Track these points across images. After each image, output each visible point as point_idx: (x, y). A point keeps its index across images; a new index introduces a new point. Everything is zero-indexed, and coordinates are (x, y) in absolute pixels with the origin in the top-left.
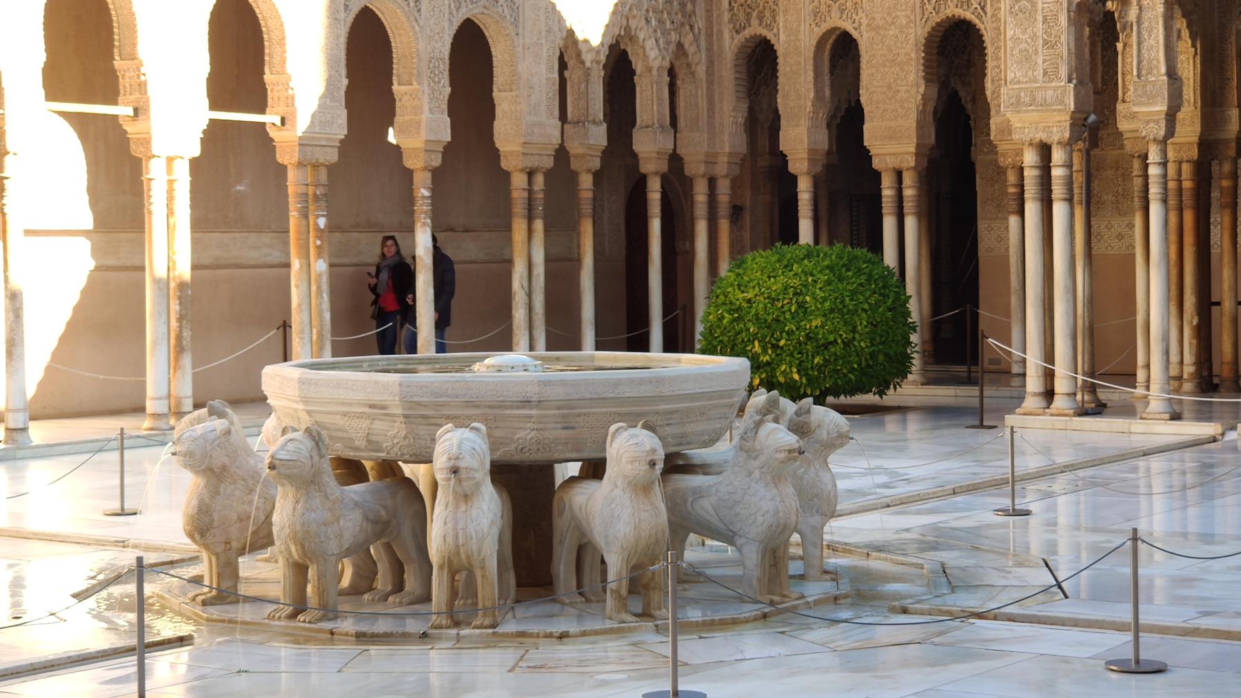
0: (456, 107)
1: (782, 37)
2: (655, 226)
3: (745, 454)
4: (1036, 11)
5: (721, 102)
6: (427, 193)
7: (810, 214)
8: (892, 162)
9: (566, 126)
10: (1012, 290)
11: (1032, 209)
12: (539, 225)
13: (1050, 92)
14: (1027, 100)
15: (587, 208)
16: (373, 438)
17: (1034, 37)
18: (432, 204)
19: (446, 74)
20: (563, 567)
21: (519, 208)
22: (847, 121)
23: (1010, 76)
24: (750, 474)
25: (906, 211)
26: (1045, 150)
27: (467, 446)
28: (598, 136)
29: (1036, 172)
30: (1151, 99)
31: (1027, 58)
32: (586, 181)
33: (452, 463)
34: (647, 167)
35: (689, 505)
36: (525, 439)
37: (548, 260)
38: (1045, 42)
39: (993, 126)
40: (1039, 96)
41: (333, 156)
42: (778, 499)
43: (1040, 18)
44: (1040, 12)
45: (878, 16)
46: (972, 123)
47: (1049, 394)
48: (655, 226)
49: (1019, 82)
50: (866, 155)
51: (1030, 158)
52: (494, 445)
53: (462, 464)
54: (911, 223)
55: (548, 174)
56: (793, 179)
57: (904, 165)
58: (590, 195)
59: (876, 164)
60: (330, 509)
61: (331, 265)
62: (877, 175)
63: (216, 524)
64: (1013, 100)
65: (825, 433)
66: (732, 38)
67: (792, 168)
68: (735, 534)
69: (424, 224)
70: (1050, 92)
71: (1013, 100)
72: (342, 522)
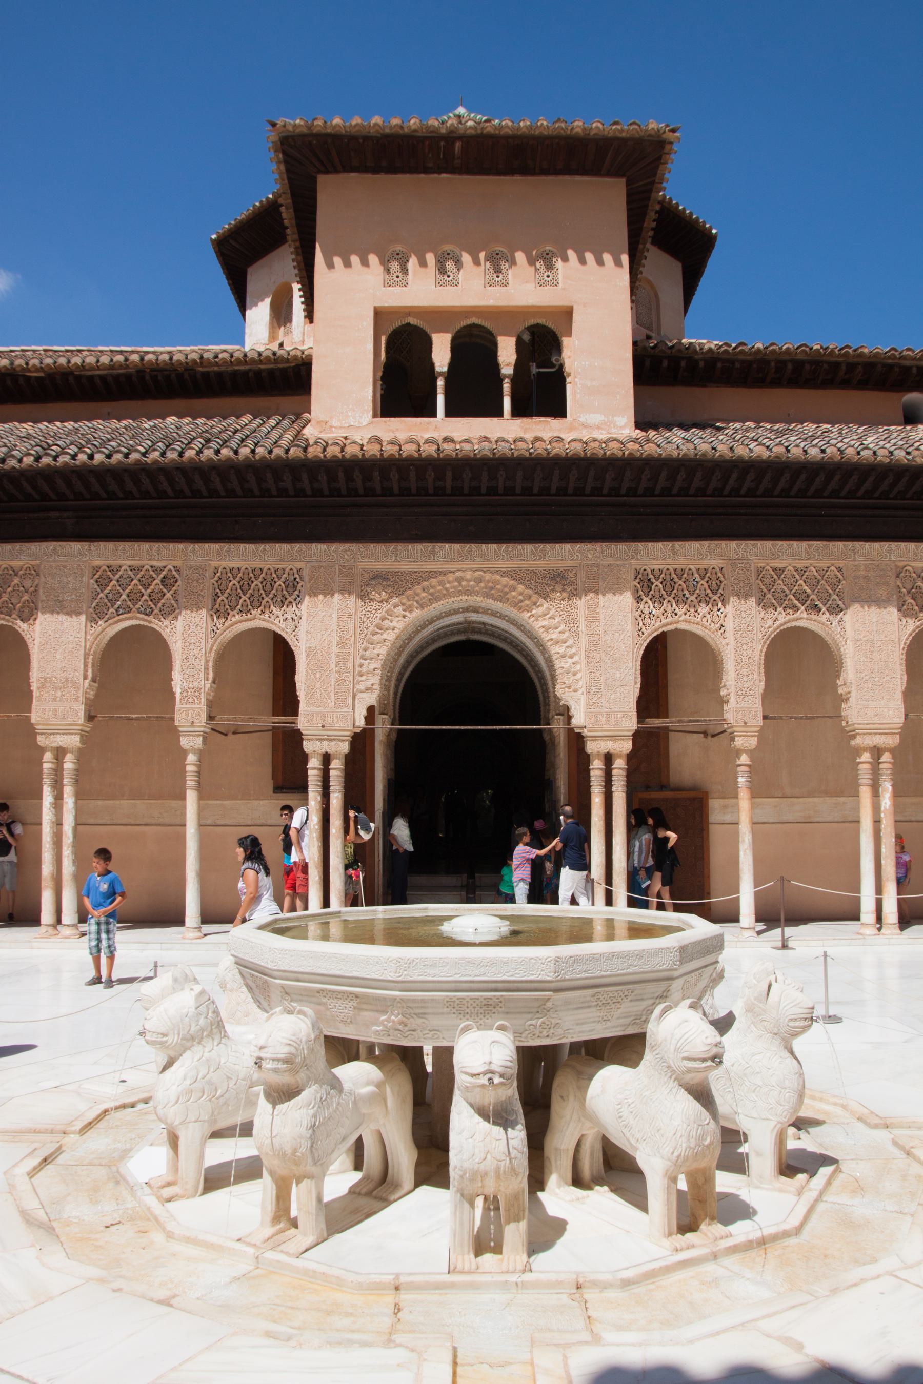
65: (672, 1048)
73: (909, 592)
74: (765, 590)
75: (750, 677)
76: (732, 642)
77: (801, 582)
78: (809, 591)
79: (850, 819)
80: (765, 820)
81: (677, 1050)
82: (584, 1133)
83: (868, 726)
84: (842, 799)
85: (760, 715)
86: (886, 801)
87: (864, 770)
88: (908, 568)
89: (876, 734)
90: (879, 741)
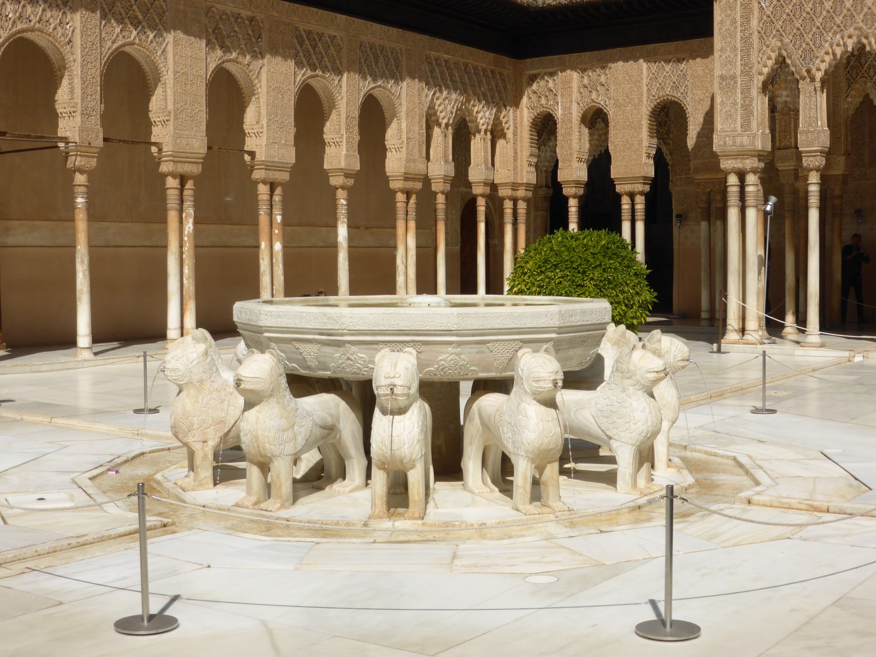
0: (363, 147)
1: (560, 111)
2: (482, 227)
3: (620, 375)
4: (736, 87)
5: (522, 152)
6: (344, 202)
7: (576, 220)
8: (627, 188)
9: (429, 164)
10: (703, 267)
11: (733, 214)
12: (412, 224)
13: (745, 138)
15: (441, 215)
16: (322, 359)
17: (735, 103)
18: (348, 210)
19: (357, 128)
20: (471, 463)
21: (400, 213)
22: (600, 163)
24: (624, 390)
25: (636, 218)
26: (742, 176)
27: (400, 369)
28: (450, 170)
31: (729, 116)
32: (441, 199)
33: (388, 382)
34: (477, 190)
35: (572, 415)
36: (445, 361)
37: (418, 247)
41: (285, 176)
42: (647, 410)
43: (739, 91)
44: (739, 86)
45: (620, 99)
46: (670, 167)
47: (743, 331)
48: (482, 227)
49: (724, 131)
50: (611, 184)
51: (733, 180)
52: (421, 366)
53: (398, 382)
54: (640, 227)
55: (419, 194)
56: (566, 199)
57: (636, 190)
58: (443, 206)
59: (619, 189)
60: (286, 418)
61: (284, 247)
62: (618, 197)
63: (195, 426)
64: (721, 143)
66: (529, 113)
67: (566, 191)
68: (610, 438)
69: (343, 222)
70: (745, 138)
72: (296, 427)
73: (213, 32)
74: (107, 10)
75: (93, 97)
76: (79, 60)
77: (135, 7)
78: (140, 17)
79: (112, 243)
80: (43, 244)
81: (674, 357)
82: (487, 444)
83: (180, 155)
84: (105, 224)
85: (101, 136)
86: (189, 226)
87: (172, 195)
88: (213, 9)
89: (186, 162)
90: (187, 169)
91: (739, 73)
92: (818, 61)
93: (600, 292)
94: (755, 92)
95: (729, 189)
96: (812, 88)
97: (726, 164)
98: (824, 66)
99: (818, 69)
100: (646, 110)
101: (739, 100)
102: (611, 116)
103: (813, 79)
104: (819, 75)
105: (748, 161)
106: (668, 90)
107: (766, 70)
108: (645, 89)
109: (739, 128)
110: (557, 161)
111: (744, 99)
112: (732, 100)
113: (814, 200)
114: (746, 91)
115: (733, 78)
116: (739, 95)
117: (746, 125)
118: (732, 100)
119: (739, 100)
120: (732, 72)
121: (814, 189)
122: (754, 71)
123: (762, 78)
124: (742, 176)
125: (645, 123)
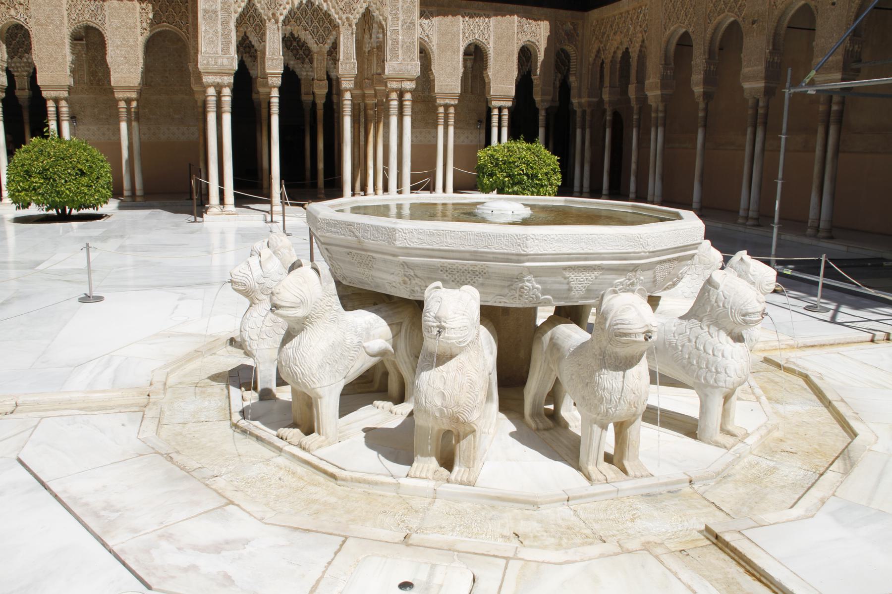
8: (54, 94)
11: (212, 118)
13: (225, 60)
14: (213, 63)
23: (203, 50)
26: (219, 88)
29: (214, 98)
30: (275, 68)
38: (222, 35)
39: (112, 79)
40: (219, 61)
43: (219, 23)
57: (62, 96)
59: (45, 94)
64: (205, 62)
70: (225, 60)
71: (205, 62)
91: (219, 8)
92: (281, 8)
93: (675, 198)
94: (232, 25)
95: (209, 98)
96: (275, 27)
97: (207, 79)
98: (285, 12)
99: (281, 14)
100: (66, 32)
101: (219, 30)
102: (33, 33)
103: (277, 22)
104: (281, 18)
105: (226, 78)
106: (87, 17)
107: (240, 10)
108: (66, 13)
109: (220, 52)
110: (35, 70)
111: (223, 29)
112: (214, 28)
113: (275, 109)
114: (225, 24)
115: (215, 12)
116: (220, 26)
117: (225, 50)
118: (214, 28)
119: (219, 30)
120: (213, 8)
121: (275, 101)
122: (232, 9)
123: (237, 15)
124: (219, 88)
125: (67, 41)
